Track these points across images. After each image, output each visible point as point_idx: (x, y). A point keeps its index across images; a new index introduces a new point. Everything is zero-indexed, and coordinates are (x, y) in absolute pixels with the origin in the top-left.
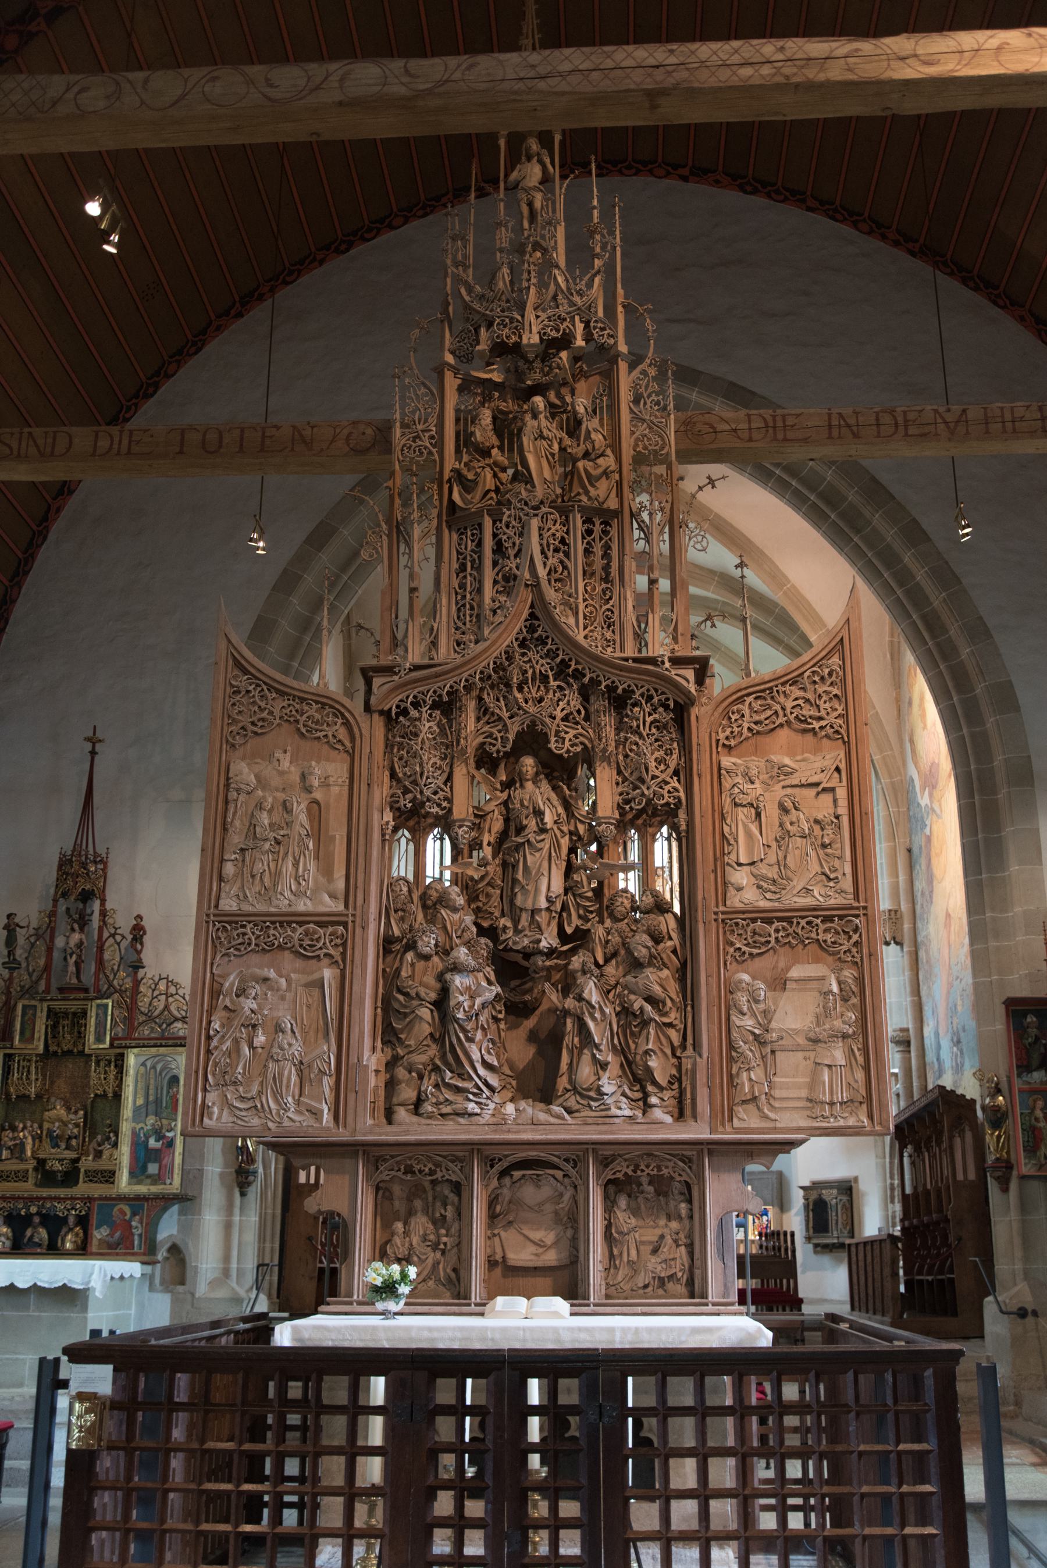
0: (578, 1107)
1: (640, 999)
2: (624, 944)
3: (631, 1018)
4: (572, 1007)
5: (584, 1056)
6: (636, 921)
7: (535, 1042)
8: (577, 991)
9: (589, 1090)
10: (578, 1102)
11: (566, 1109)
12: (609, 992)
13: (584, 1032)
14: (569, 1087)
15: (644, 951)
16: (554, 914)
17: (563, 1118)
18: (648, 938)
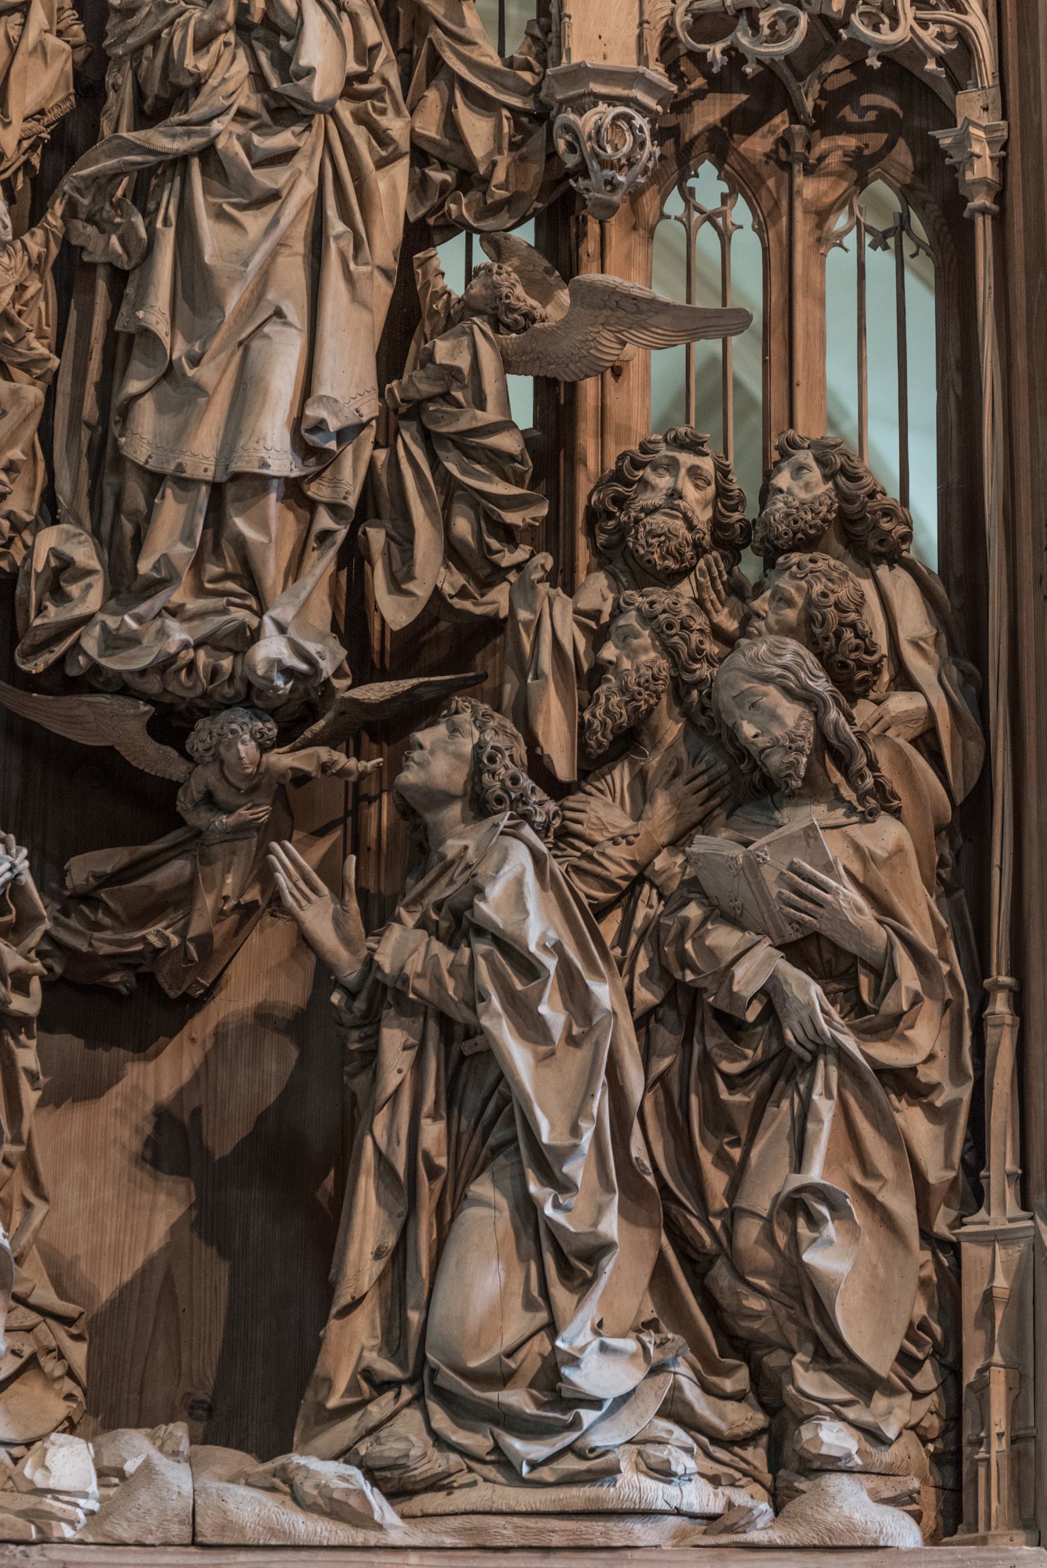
0: (440, 1462)
1: (764, 949)
2: (679, 690)
3: (714, 1040)
4: (415, 965)
5: (471, 1213)
6: (737, 590)
7: (181, 1168)
8: (442, 891)
9: (502, 1378)
10: (439, 1441)
11: (370, 1473)
12: (602, 911)
13: (472, 1099)
14: (388, 1369)
15: (791, 713)
16: (325, 520)
17: (363, 1520)
18: (811, 660)
